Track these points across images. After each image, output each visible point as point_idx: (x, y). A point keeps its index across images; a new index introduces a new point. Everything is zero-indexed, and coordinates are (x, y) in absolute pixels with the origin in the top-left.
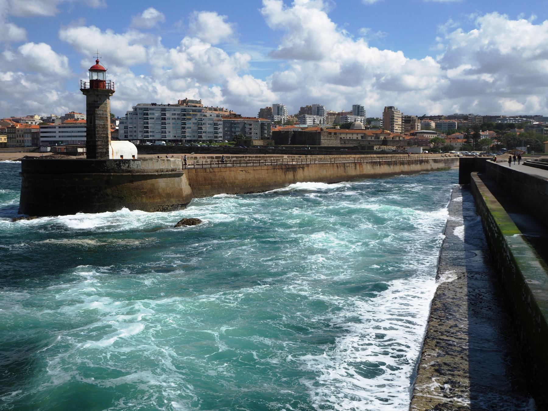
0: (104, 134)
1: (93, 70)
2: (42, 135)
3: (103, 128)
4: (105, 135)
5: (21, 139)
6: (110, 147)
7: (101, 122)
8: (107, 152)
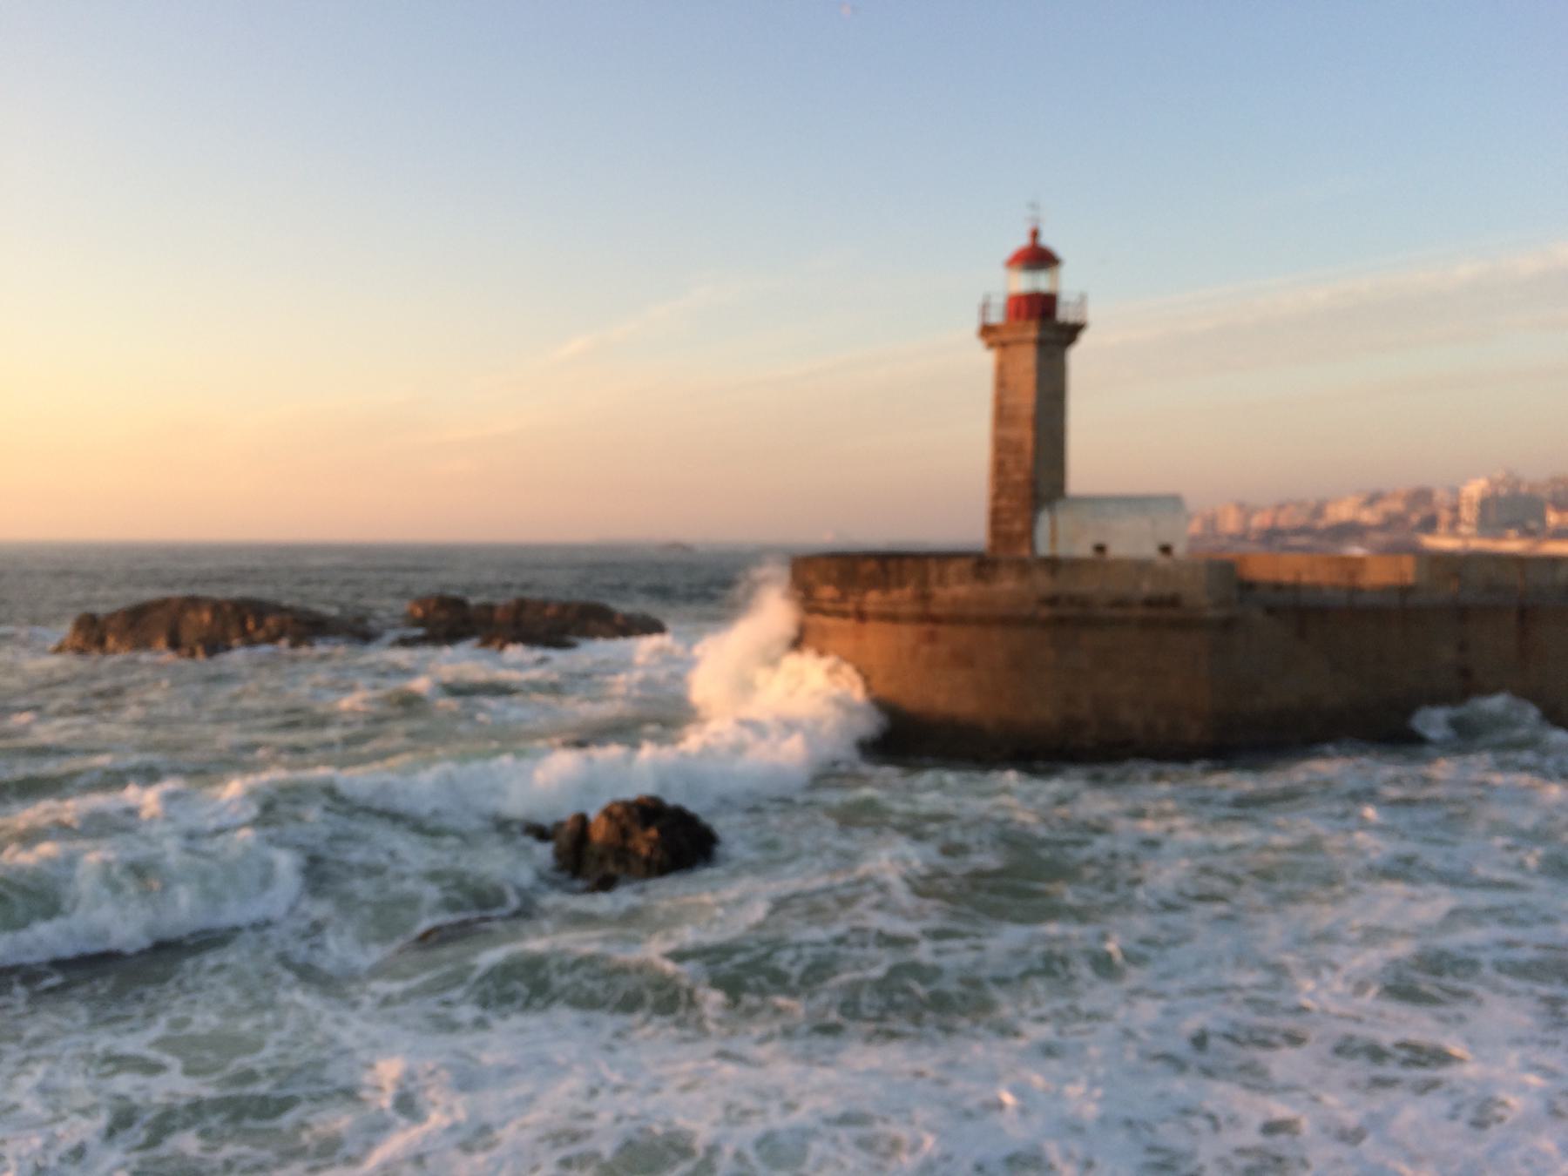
8: (1029, 533)
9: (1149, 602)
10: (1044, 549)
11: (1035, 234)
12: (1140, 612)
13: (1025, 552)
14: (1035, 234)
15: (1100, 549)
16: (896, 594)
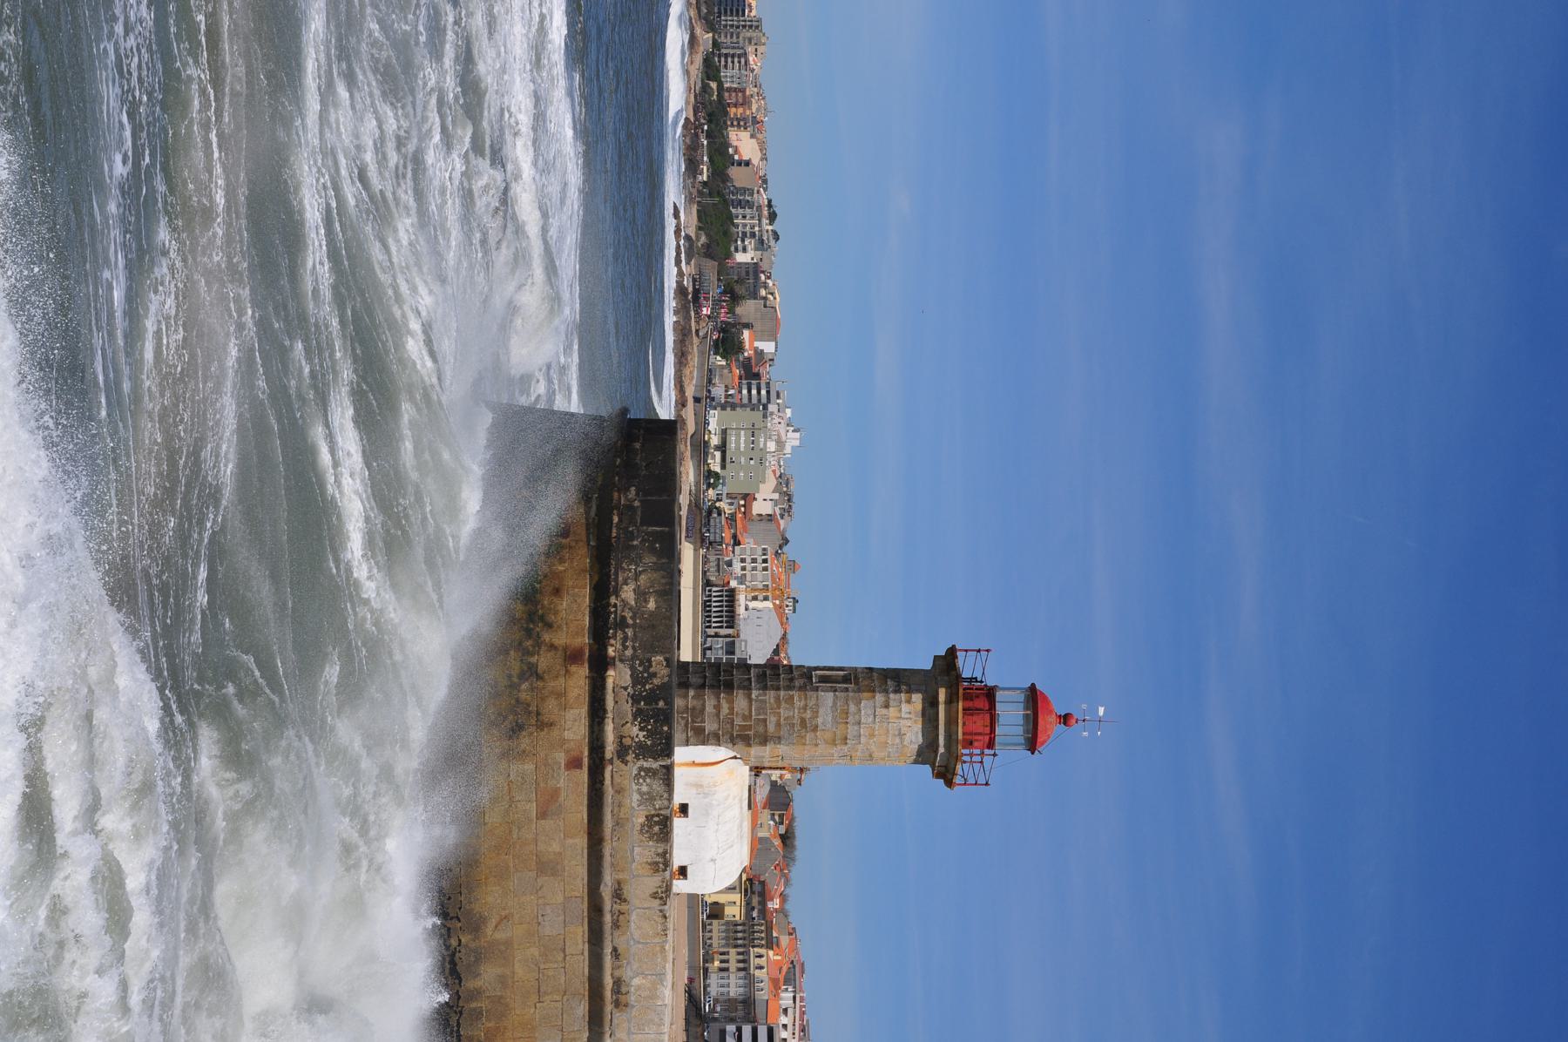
0: (778, 725)
1: (1033, 698)
2: (747, 1030)
3: (803, 721)
4: (771, 728)
5: (733, 965)
6: (722, 752)
7: (825, 717)
8: (701, 737)
9: (618, 983)
10: (681, 754)
11: (1066, 719)
12: (608, 982)
13: (678, 736)
14: (1066, 719)
15: (684, 809)
16: (628, 708)
